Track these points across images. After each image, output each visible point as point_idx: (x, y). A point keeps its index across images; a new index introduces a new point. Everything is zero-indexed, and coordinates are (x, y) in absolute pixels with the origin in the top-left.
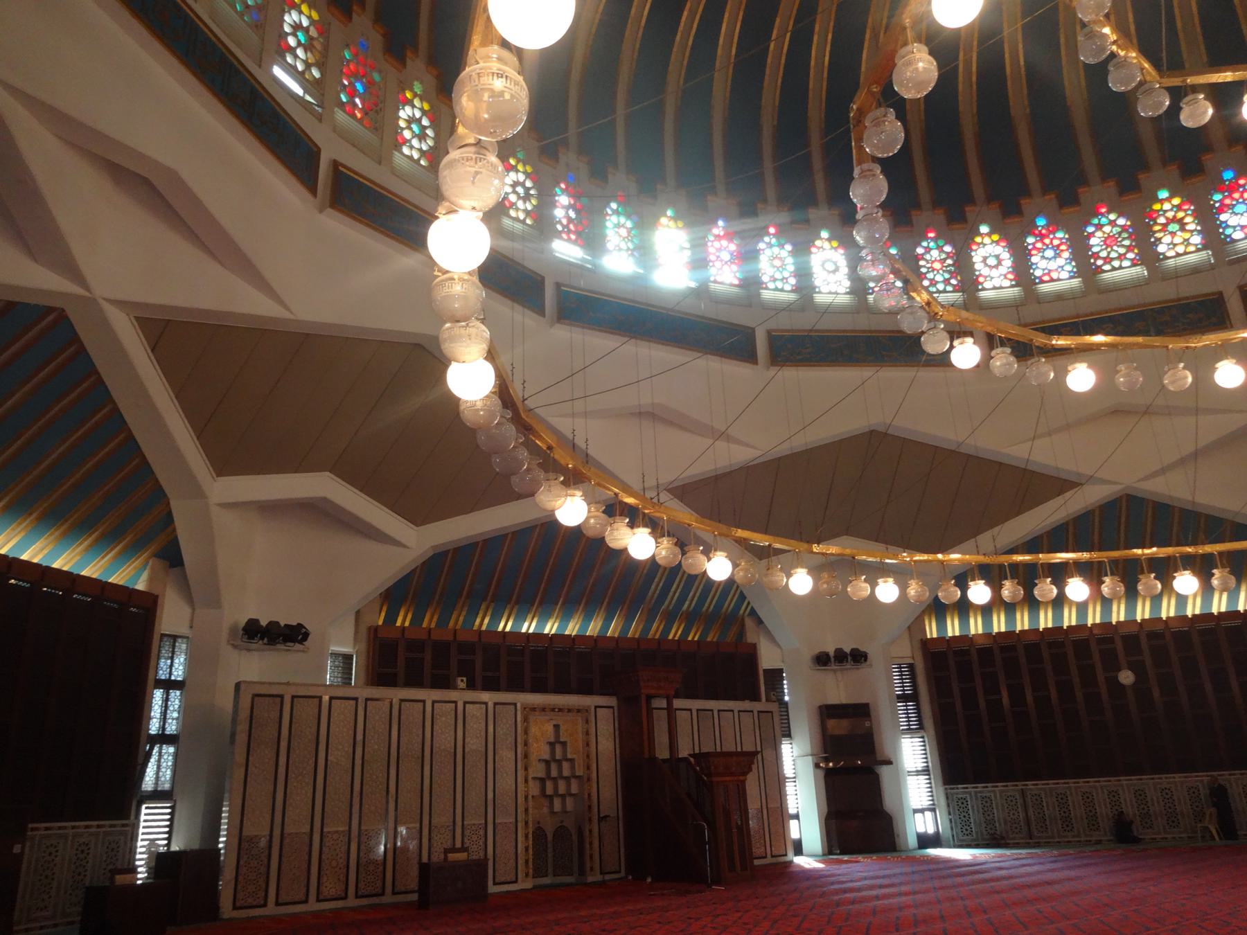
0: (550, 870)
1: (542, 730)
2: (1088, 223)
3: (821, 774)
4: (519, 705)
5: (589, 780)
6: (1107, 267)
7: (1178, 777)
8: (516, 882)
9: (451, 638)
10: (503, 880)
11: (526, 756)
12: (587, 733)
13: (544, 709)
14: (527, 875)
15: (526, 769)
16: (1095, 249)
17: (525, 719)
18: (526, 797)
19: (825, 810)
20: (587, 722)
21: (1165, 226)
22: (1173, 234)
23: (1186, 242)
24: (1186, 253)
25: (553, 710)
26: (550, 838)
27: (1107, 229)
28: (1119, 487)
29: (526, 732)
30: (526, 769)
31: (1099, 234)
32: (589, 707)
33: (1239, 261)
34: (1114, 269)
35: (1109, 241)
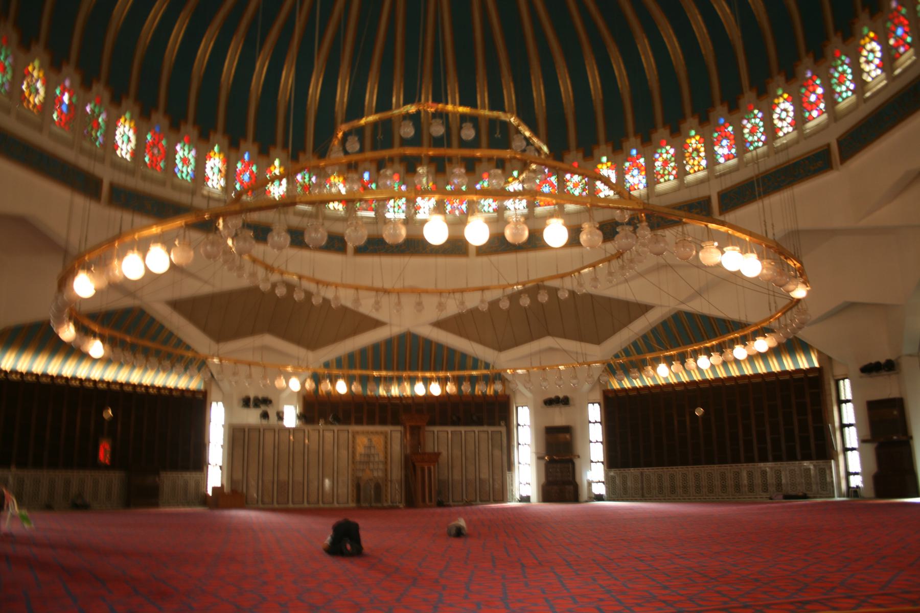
1: (362, 442)
2: (656, 152)
3: (543, 463)
6: (662, 180)
7: (716, 467)
16: (658, 169)
19: (543, 480)
21: (691, 154)
22: (694, 159)
23: (699, 165)
24: (699, 170)
27: (665, 156)
28: (667, 309)
29: (353, 442)
31: (660, 159)
33: (721, 175)
34: (665, 181)
35: (666, 163)
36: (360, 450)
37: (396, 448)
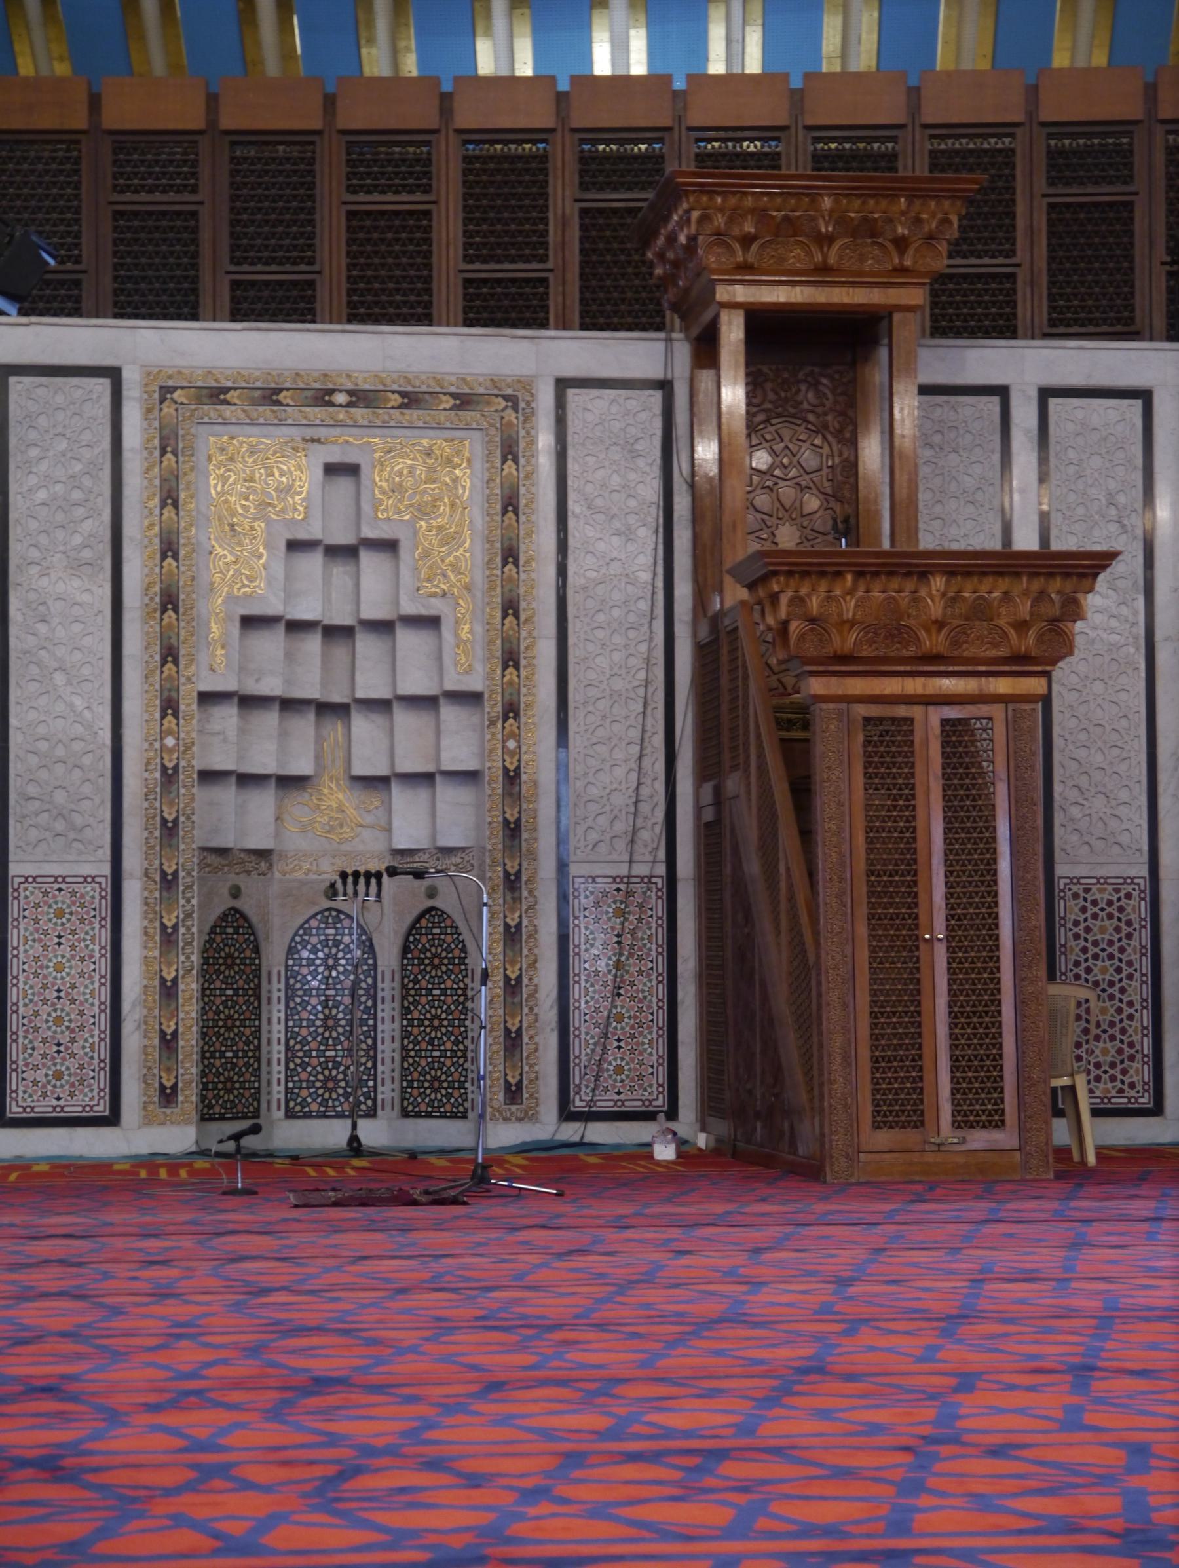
0: (387, 1092)
4: (130, 376)
5: (512, 710)
8: (112, 1119)
9: (79, 120)
10: (44, 1108)
11: (169, 601)
12: (511, 504)
13: (271, 396)
14: (168, 1096)
15: (170, 654)
17: (167, 442)
18: (169, 776)
20: (510, 451)
25: (323, 398)
26: (388, 957)
29: (170, 498)
30: (170, 654)
32: (527, 384)
36: (238, 568)
37: (618, 562)
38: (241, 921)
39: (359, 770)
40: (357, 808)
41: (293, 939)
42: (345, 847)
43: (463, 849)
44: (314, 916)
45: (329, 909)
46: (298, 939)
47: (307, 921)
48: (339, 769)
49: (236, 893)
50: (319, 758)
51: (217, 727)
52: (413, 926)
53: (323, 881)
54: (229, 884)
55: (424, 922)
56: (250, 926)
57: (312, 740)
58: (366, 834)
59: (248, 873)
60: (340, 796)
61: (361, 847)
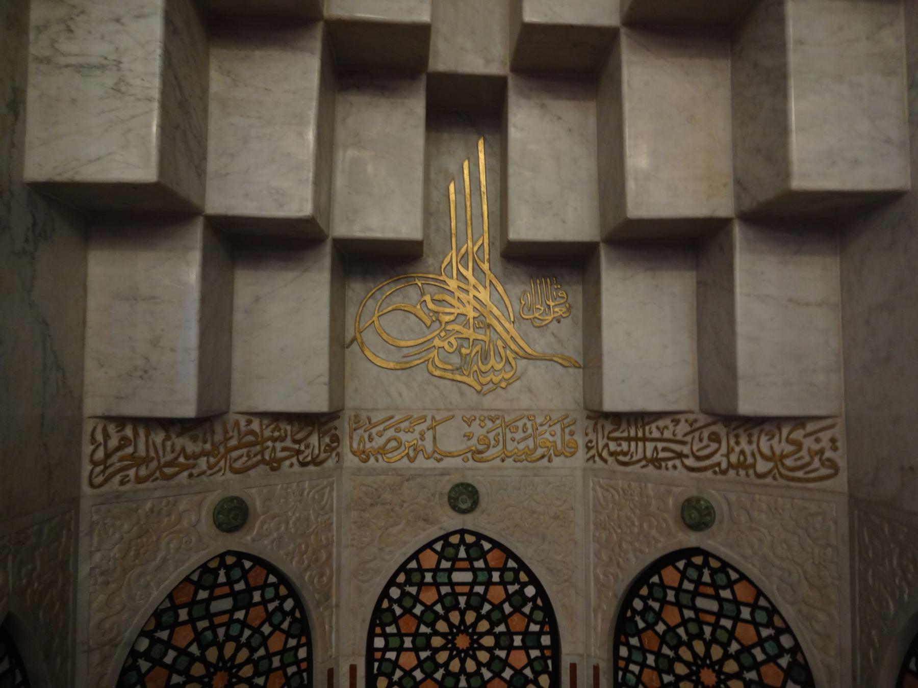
38: (258, 576)
39: (526, 227)
40: (517, 320)
41: (385, 594)
42: (492, 402)
43: (799, 421)
44: (429, 545)
45: (462, 532)
46: (395, 593)
47: (415, 556)
48: (481, 241)
49: (233, 515)
50: (432, 212)
51: (97, 50)
52: (643, 578)
53: (445, 472)
54: (213, 498)
55: (670, 576)
56: (283, 579)
57: (419, 173)
58: (537, 374)
59: (274, 465)
60: (484, 295)
61: (525, 401)
